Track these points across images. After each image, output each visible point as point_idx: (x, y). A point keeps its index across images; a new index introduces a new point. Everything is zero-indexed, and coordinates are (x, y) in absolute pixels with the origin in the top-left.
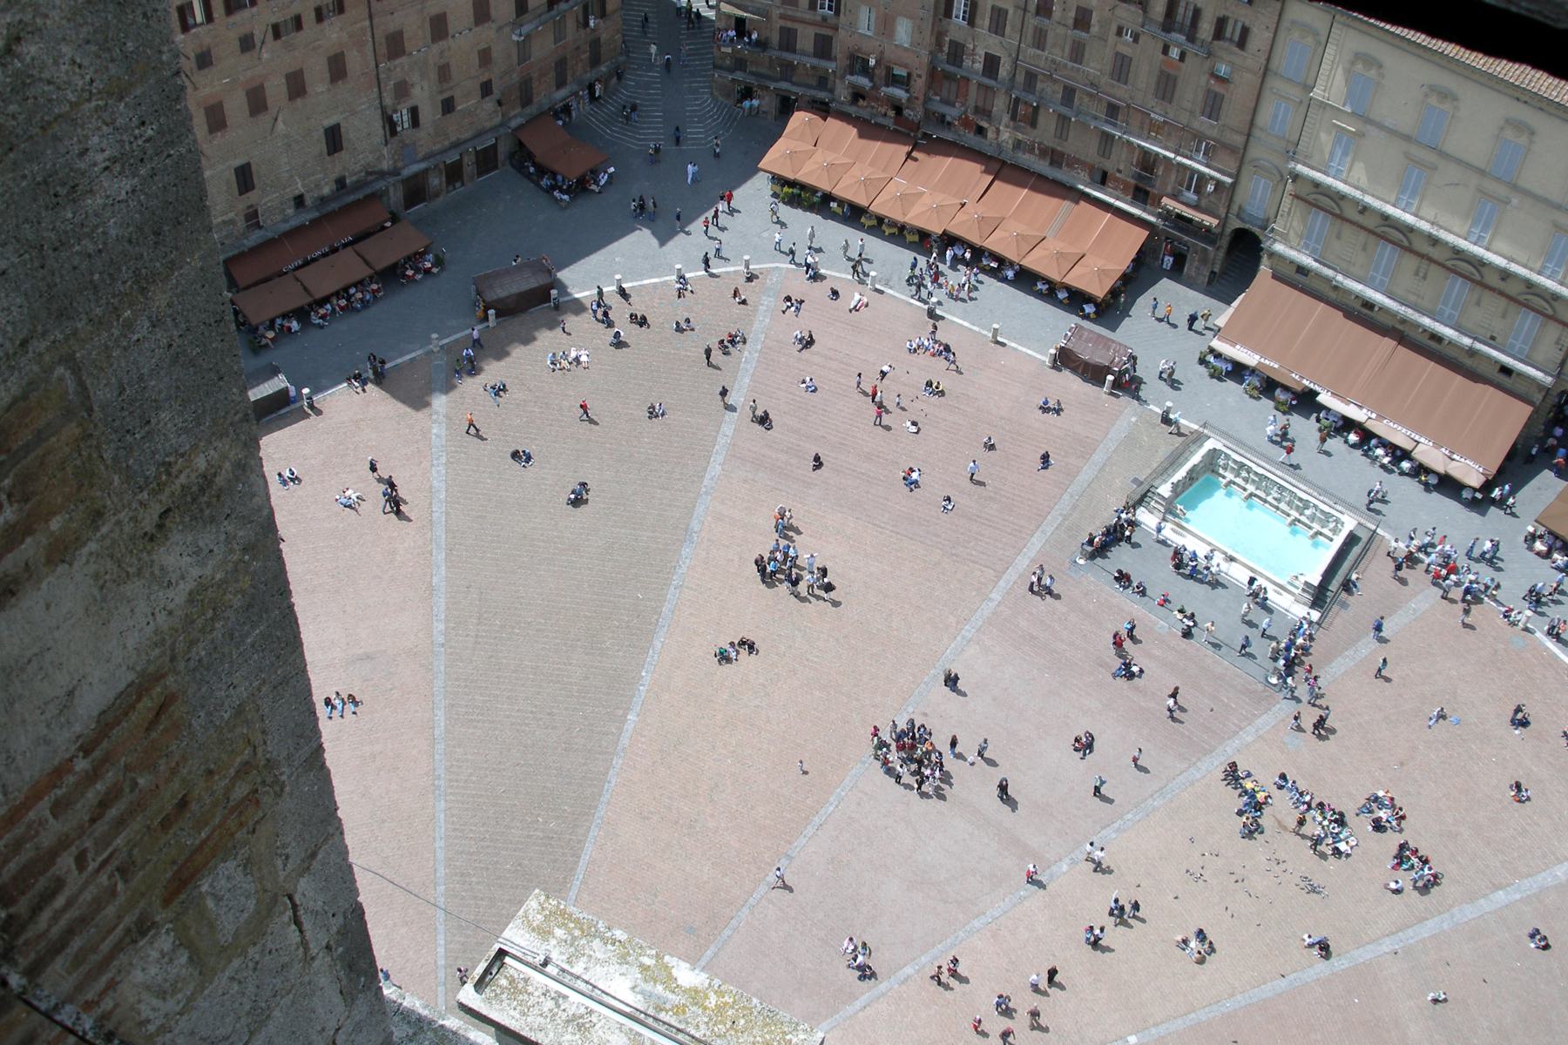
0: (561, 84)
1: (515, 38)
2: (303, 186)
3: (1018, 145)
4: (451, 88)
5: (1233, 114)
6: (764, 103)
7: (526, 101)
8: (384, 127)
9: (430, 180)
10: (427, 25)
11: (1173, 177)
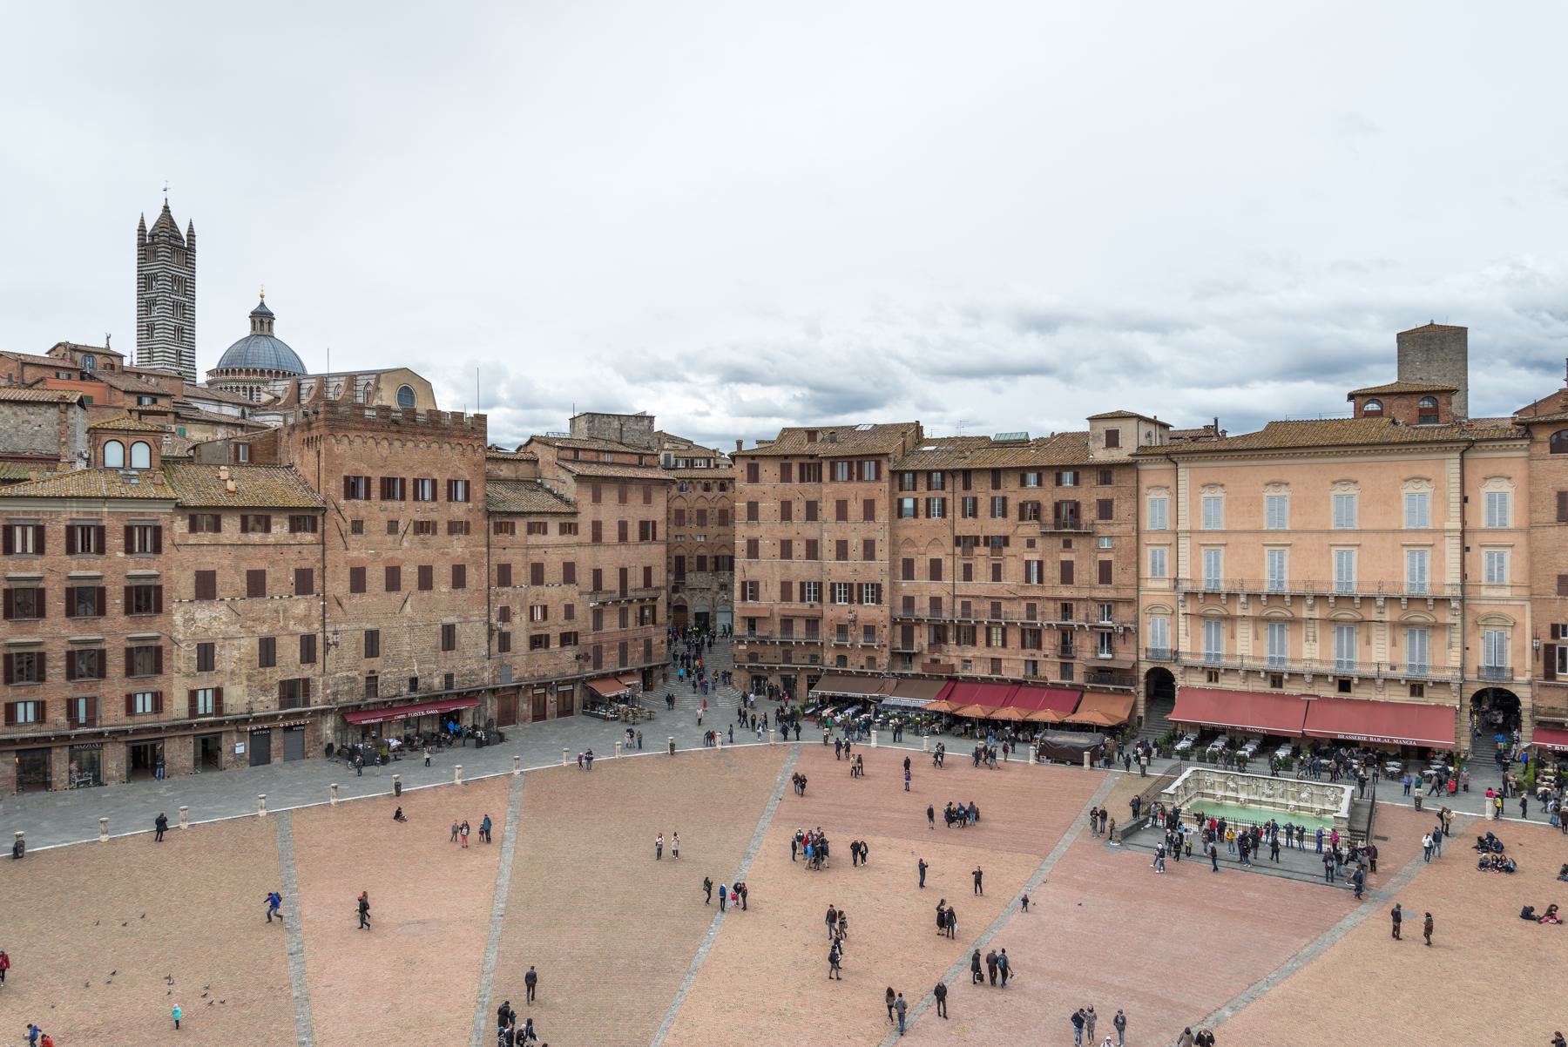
2: (419, 671)
9: (521, 703)
10: (529, 569)
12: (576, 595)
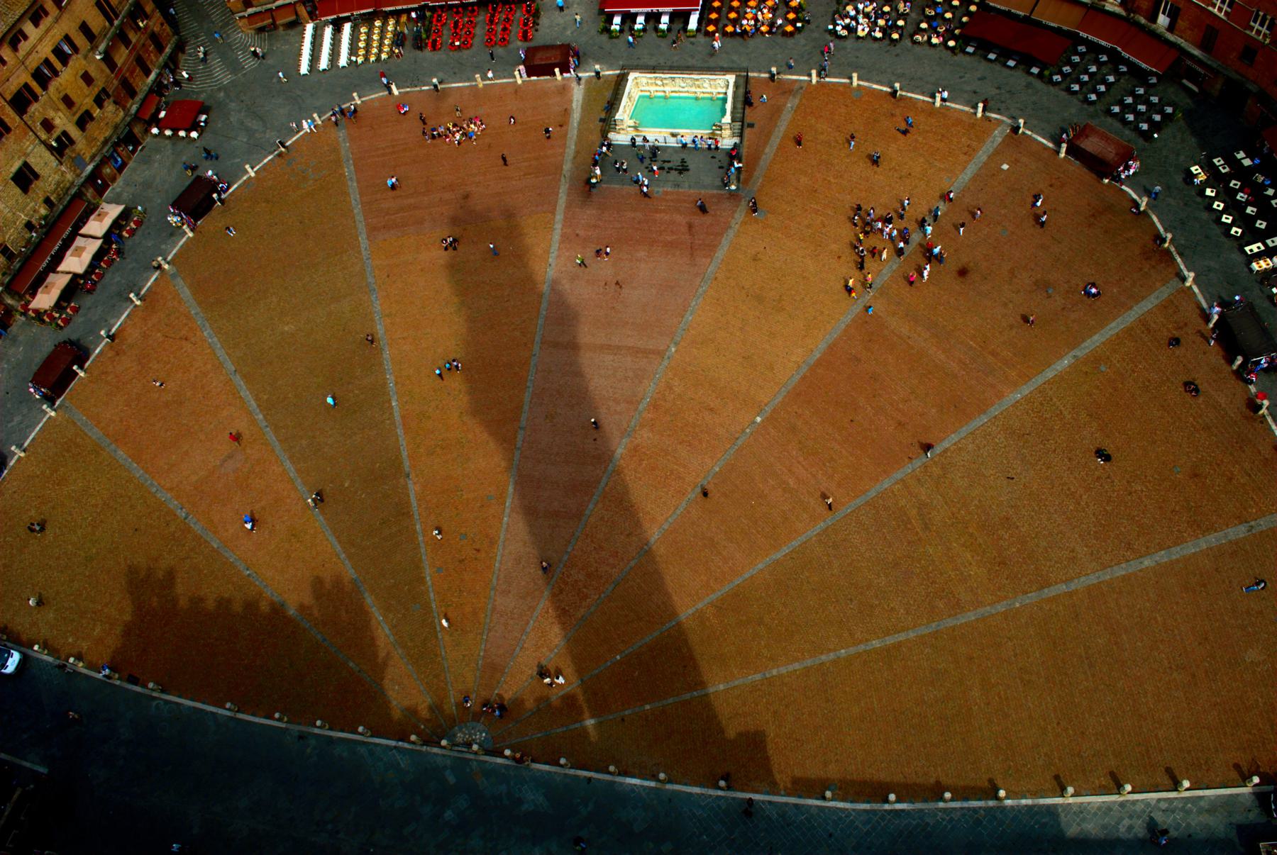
0: (148, 73)
1: (98, 57)
2: (26, 215)
4: (79, 109)
6: (151, 23)
7: (132, 93)
8: (52, 154)
12: (84, 62)
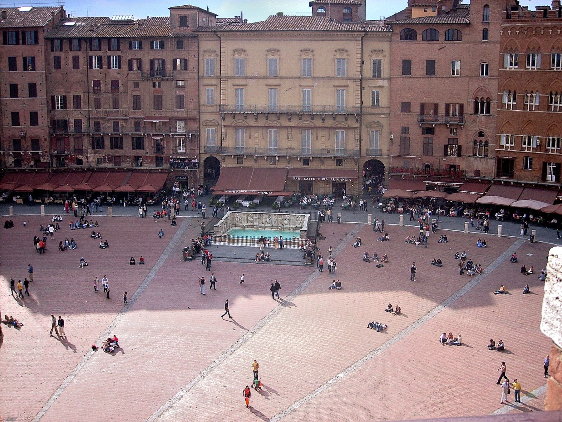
3: (99, 160)
5: (190, 105)
11: (172, 145)
